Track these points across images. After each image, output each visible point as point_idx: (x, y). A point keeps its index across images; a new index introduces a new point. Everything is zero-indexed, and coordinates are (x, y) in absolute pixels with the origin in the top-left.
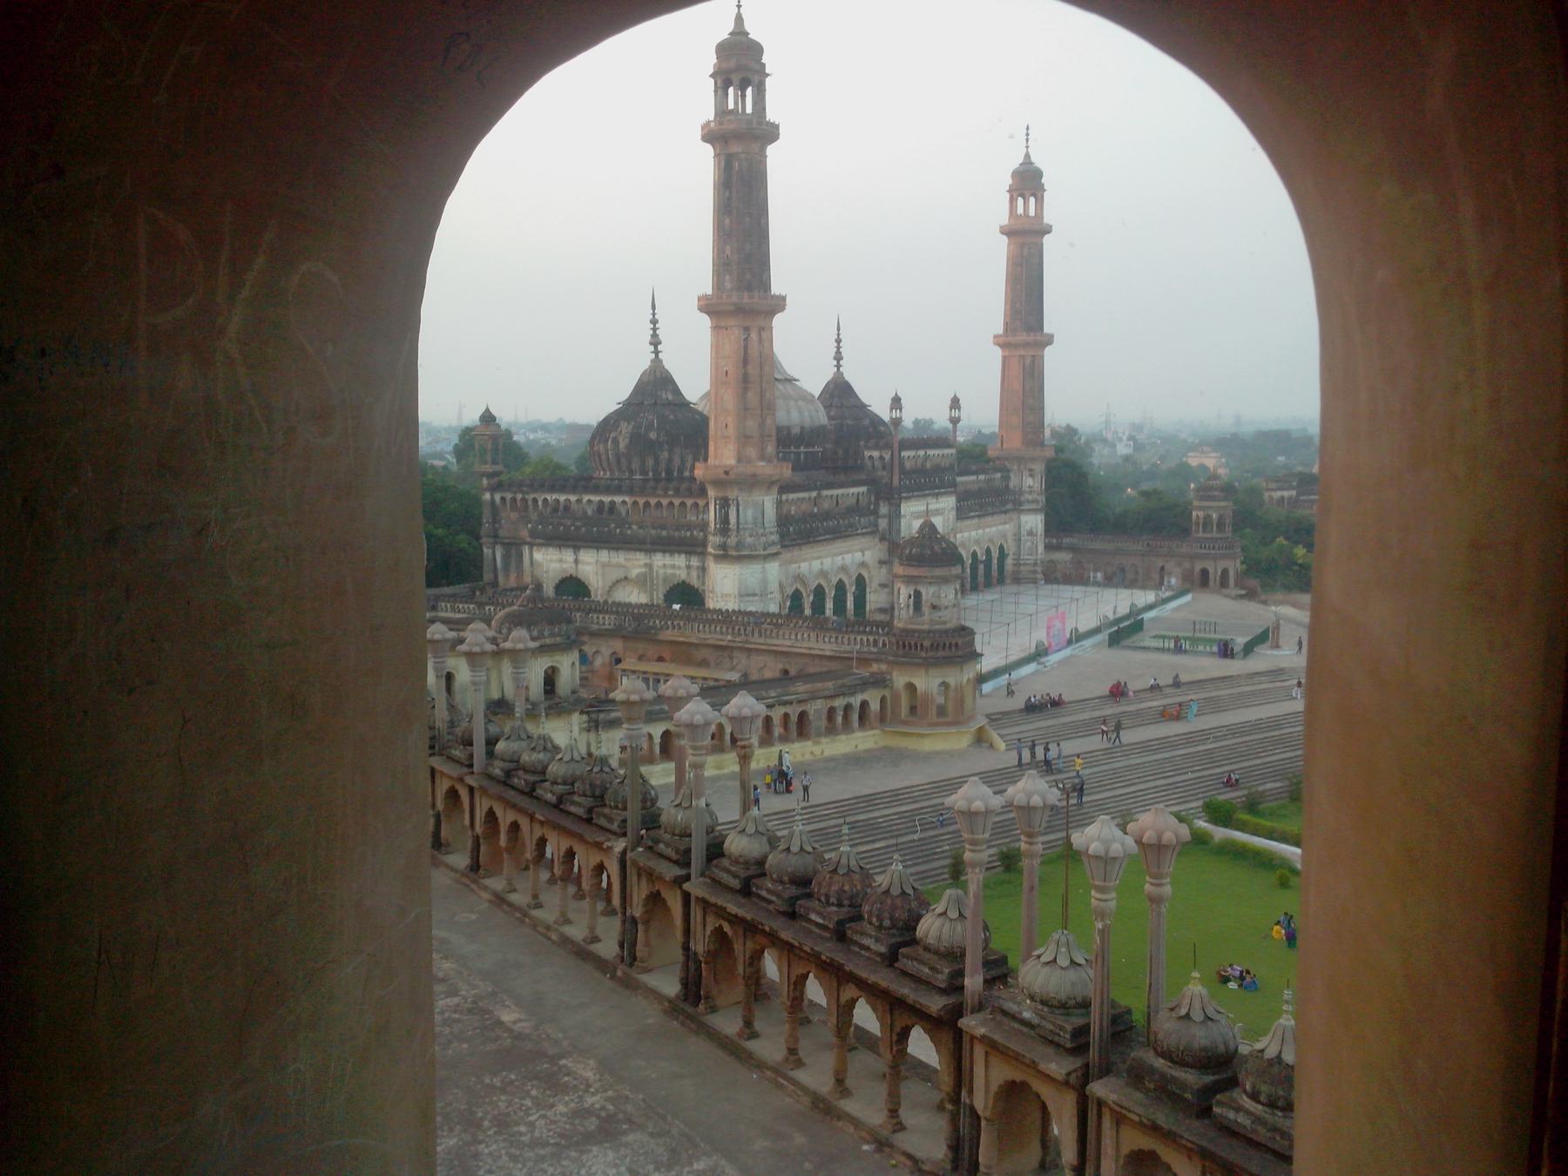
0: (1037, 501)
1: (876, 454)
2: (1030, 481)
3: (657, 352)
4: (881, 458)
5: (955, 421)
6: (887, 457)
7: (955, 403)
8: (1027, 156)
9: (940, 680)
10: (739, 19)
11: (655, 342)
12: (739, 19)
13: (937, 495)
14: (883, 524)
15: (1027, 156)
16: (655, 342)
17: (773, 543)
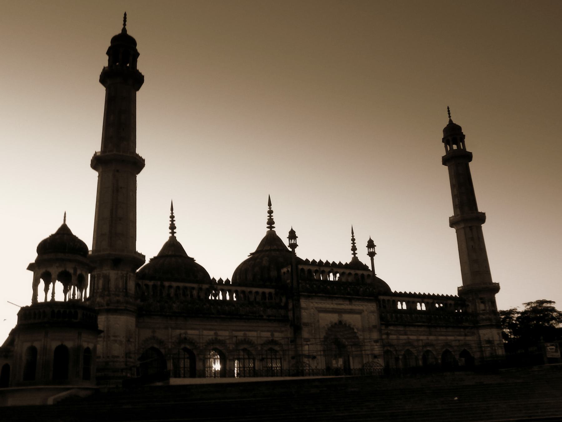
0: (490, 320)
1: (285, 270)
2: (482, 306)
3: (173, 233)
4: (288, 271)
5: (372, 255)
6: (290, 269)
7: (371, 244)
8: (451, 121)
9: (27, 345)
10: (124, 30)
11: (173, 227)
12: (124, 30)
13: (350, 300)
14: (290, 314)
15: (451, 121)
16: (173, 227)
17: (118, 302)
